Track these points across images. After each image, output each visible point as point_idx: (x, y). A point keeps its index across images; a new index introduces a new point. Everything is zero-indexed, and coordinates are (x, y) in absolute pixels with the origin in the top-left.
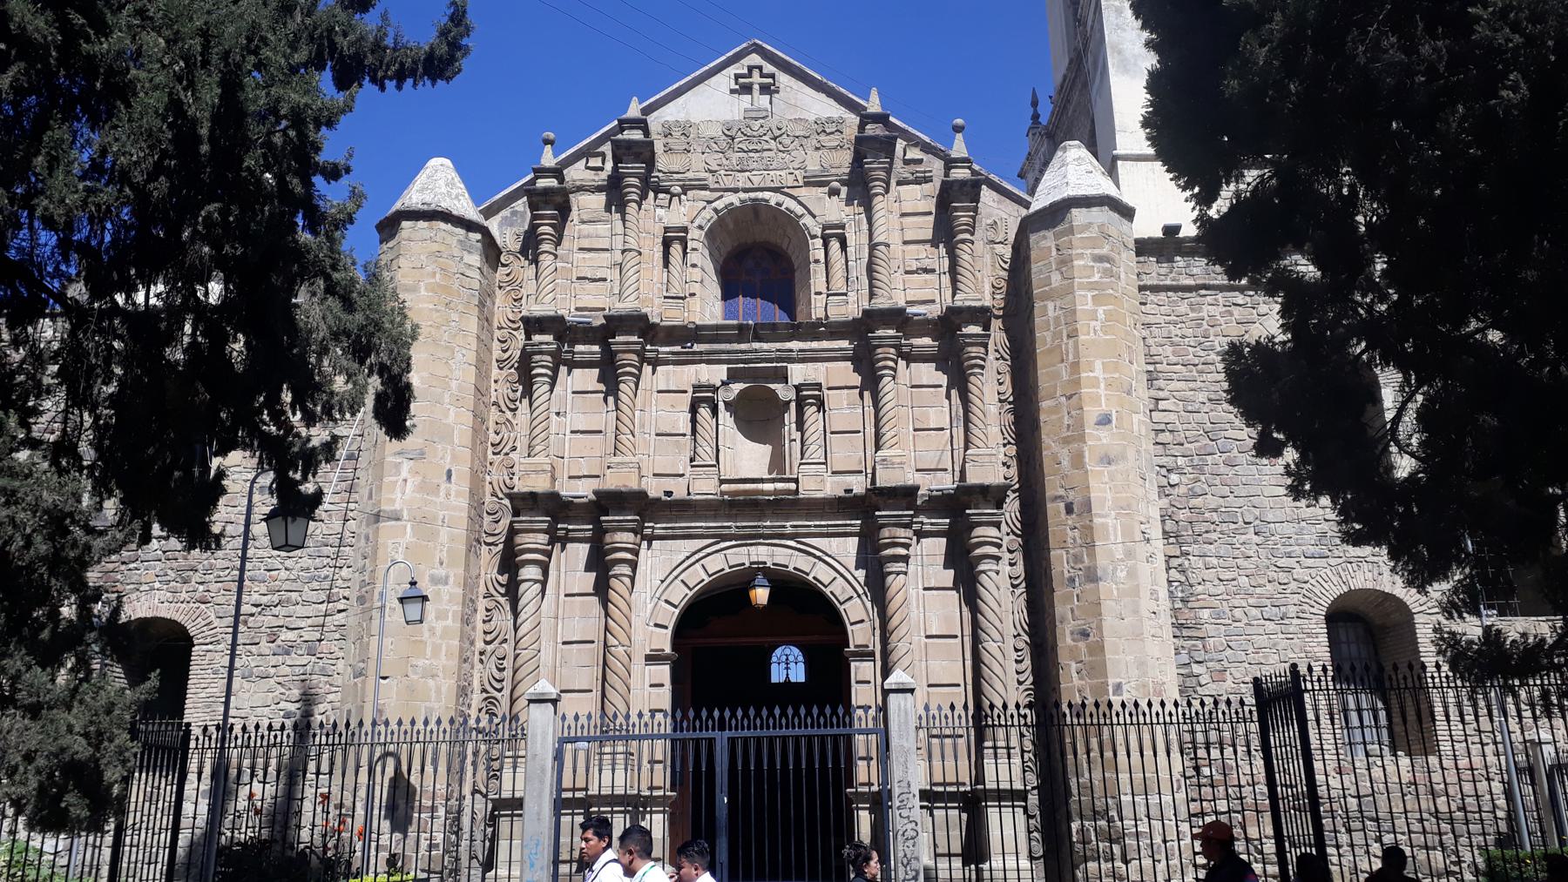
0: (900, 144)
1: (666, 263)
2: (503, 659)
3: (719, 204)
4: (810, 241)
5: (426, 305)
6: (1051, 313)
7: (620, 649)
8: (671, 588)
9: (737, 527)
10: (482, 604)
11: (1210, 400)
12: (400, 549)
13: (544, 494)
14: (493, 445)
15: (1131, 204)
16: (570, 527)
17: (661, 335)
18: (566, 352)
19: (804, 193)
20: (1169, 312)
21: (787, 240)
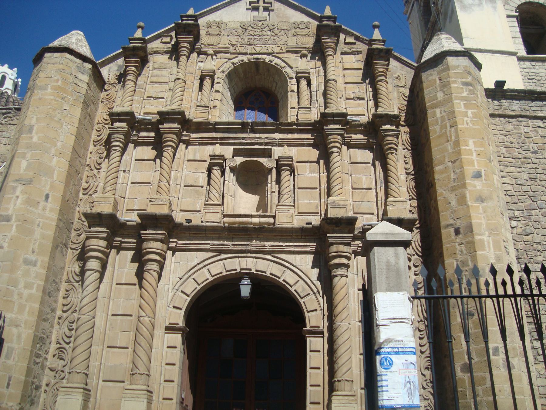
0: (342, 36)
1: (201, 89)
2: (73, 323)
3: (235, 61)
4: (289, 81)
5: (50, 97)
6: (438, 114)
7: (147, 319)
8: (185, 283)
9: (233, 245)
10: (64, 286)
11: (530, 178)
12: (7, 240)
13: (106, 215)
14: (83, 189)
15: (480, 61)
16: (123, 240)
17: (193, 127)
18: (134, 135)
19: (286, 56)
20: (502, 129)
21: (274, 84)
